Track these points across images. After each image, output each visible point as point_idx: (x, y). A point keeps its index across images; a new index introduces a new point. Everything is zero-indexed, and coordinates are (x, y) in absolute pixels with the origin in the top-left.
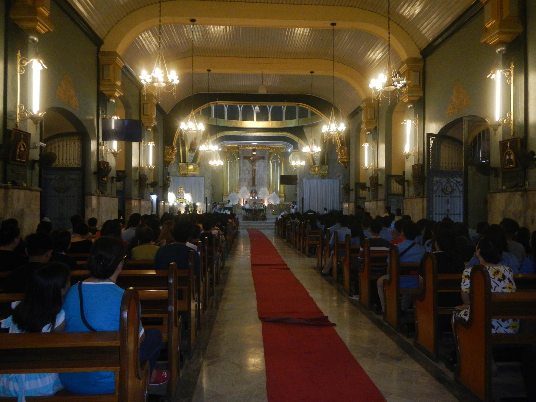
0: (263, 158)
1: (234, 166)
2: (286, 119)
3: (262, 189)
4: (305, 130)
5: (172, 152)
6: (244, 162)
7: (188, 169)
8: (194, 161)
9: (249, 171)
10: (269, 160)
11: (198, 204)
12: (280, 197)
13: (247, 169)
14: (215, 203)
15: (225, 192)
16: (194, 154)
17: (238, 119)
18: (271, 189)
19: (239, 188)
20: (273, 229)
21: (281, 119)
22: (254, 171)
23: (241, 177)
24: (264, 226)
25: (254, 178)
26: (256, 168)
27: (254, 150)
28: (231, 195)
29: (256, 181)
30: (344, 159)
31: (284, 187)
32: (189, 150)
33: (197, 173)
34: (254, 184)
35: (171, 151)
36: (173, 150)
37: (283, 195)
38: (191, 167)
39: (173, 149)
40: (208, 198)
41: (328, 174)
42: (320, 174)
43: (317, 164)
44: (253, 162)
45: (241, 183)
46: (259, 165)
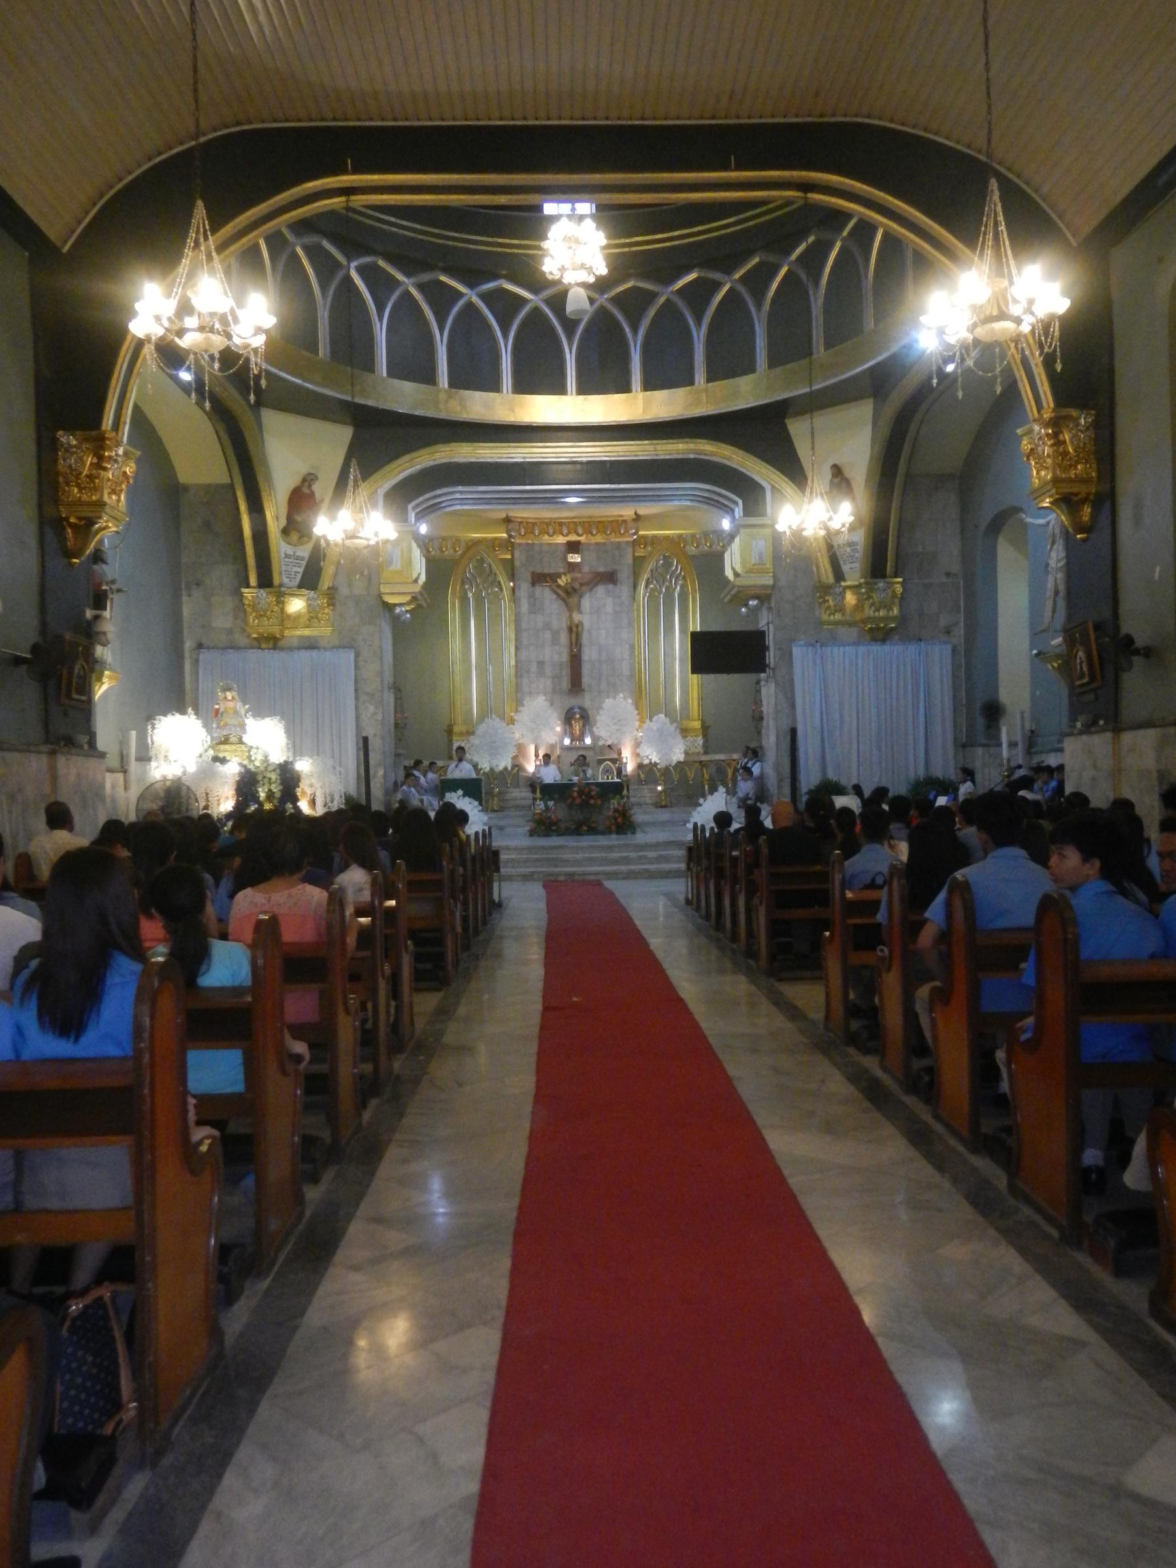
0: (610, 578)
1: (497, 616)
2: (710, 379)
3: (608, 702)
4: (797, 428)
5: (99, 466)
6: (531, 596)
7: (284, 617)
8: (310, 580)
9: (556, 634)
10: (635, 586)
11: (303, 766)
12: (684, 732)
13: (547, 626)
14: (418, 763)
15: (459, 719)
17: (494, 386)
18: (649, 703)
19: (519, 703)
20: (675, 874)
21: (690, 382)
22: (575, 632)
23: (524, 655)
24: (626, 861)
25: (575, 661)
26: (585, 618)
27: (573, 547)
28: (481, 729)
29: (586, 670)
30: (1080, 480)
31: (701, 687)
32: (285, 532)
33: (322, 631)
34: (576, 684)
35: (89, 460)
36: (101, 458)
37: (697, 724)
38: (296, 605)
39: (99, 444)
40: (375, 744)
41: (903, 619)
43: (854, 574)
44: (570, 595)
45: (525, 681)
46: (598, 611)
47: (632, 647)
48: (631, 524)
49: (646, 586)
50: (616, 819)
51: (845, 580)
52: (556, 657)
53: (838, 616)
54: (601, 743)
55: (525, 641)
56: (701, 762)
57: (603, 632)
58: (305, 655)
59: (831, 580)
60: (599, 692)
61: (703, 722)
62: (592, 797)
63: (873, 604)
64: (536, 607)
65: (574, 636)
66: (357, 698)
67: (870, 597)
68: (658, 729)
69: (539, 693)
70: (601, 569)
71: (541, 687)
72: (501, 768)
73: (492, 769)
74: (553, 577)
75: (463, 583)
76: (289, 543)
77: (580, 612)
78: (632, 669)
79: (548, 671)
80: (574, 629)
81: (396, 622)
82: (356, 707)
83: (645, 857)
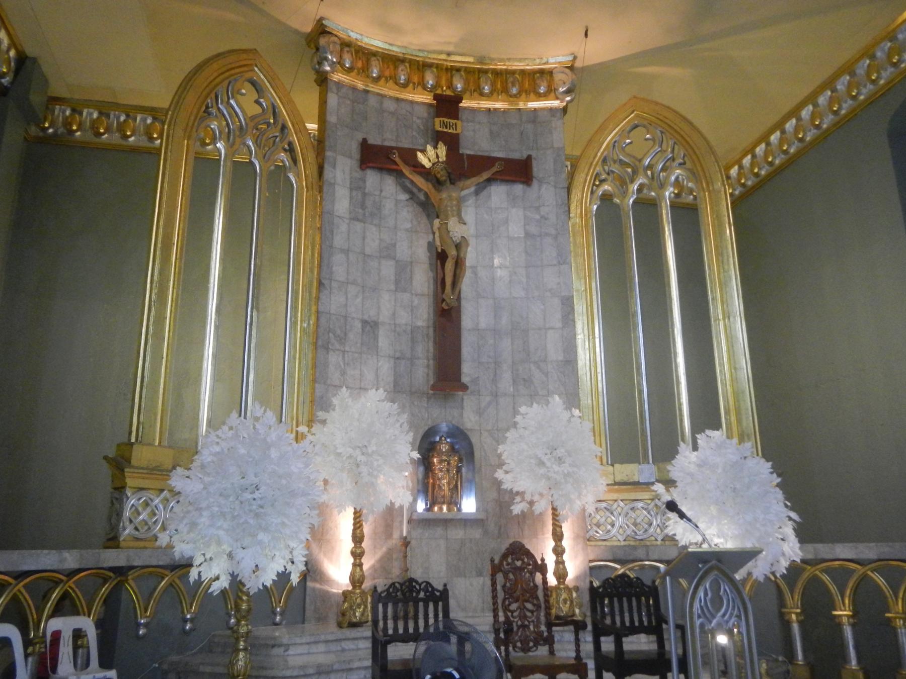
0: (519, 171)
3: (530, 414)
6: (357, 187)
9: (403, 270)
13: (387, 251)
23: (334, 302)
34: (447, 377)
48: (558, 77)
49: (592, 192)
52: (404, 318)
55: (339, 268)
60: (495, 395)
71: (370, 376)
72: (268, 578)
73: (237, 583)
79: (383, 342)
80: (452, 252)
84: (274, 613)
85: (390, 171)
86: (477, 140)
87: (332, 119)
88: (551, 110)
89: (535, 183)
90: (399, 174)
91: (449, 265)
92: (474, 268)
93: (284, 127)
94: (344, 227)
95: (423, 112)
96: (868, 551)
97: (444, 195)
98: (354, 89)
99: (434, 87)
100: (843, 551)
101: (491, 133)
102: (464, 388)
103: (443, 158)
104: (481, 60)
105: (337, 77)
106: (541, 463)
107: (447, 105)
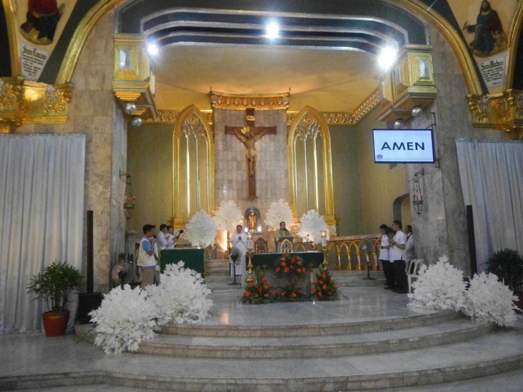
0: (273, 130)
3: (274, 204)
6: (225, 140)
9: (239, 164)
13: (234, 159)
15: (178, 215)
16: (52, 47)
23: (220, 176)
25: (252, 178)
27: (250, 112)
29: (258, 185)
32: (25, 28)
34: (252, 194)
37: (332, 218)
42: (515, 120)
44: (248, 140)
47: (287, 171)
48: (284, 99)
49: (295, 136)
50: (321, 286)
51: (488, 93)
52: (240, 178)
53: (485, 121)
54: (269, 230)
55: (221, 167)
56: (335, 241)
57: (268, 163)
58: (40, 138)
59: (480, 92)
60: (266, 199)
61: (335, 216)
62: (298, 266)
63: (517, 110)
64: (227, 147)
65: (251, 164)
66: (86, 179)
67: (514, 105)
68: (313, 218)
69: (229, 199)
70: (267, 125)
72: (207, 245)
74: (239, 129)
75: (182, 128)
76: (29, 40)
77: (255, 149)
78: (287, 185)
80: (252, 160)
81: (129, 118)
82: (86, 186)
83: (407, 340)
84: (209, 256)
85: (234, 134)
86: (260, 121)
87: (216, 120)
88: (283, 110)
89: (278, 134)
90: (236, 135)
91: (251, 164)
92: (260, 162)
93: (203, 126)
94: (221, 153)
95: (243, 113)
96: (352, 237)
97: (249, 142)
98: (222, 109)
99: (247, 105)
100: (348, 238)
101: (264, 118)
102: (257, 198)
103: (249, 130)
104: (261, 95)
105: (217, 107)
106: (275, 218)
107: (250, 112)
